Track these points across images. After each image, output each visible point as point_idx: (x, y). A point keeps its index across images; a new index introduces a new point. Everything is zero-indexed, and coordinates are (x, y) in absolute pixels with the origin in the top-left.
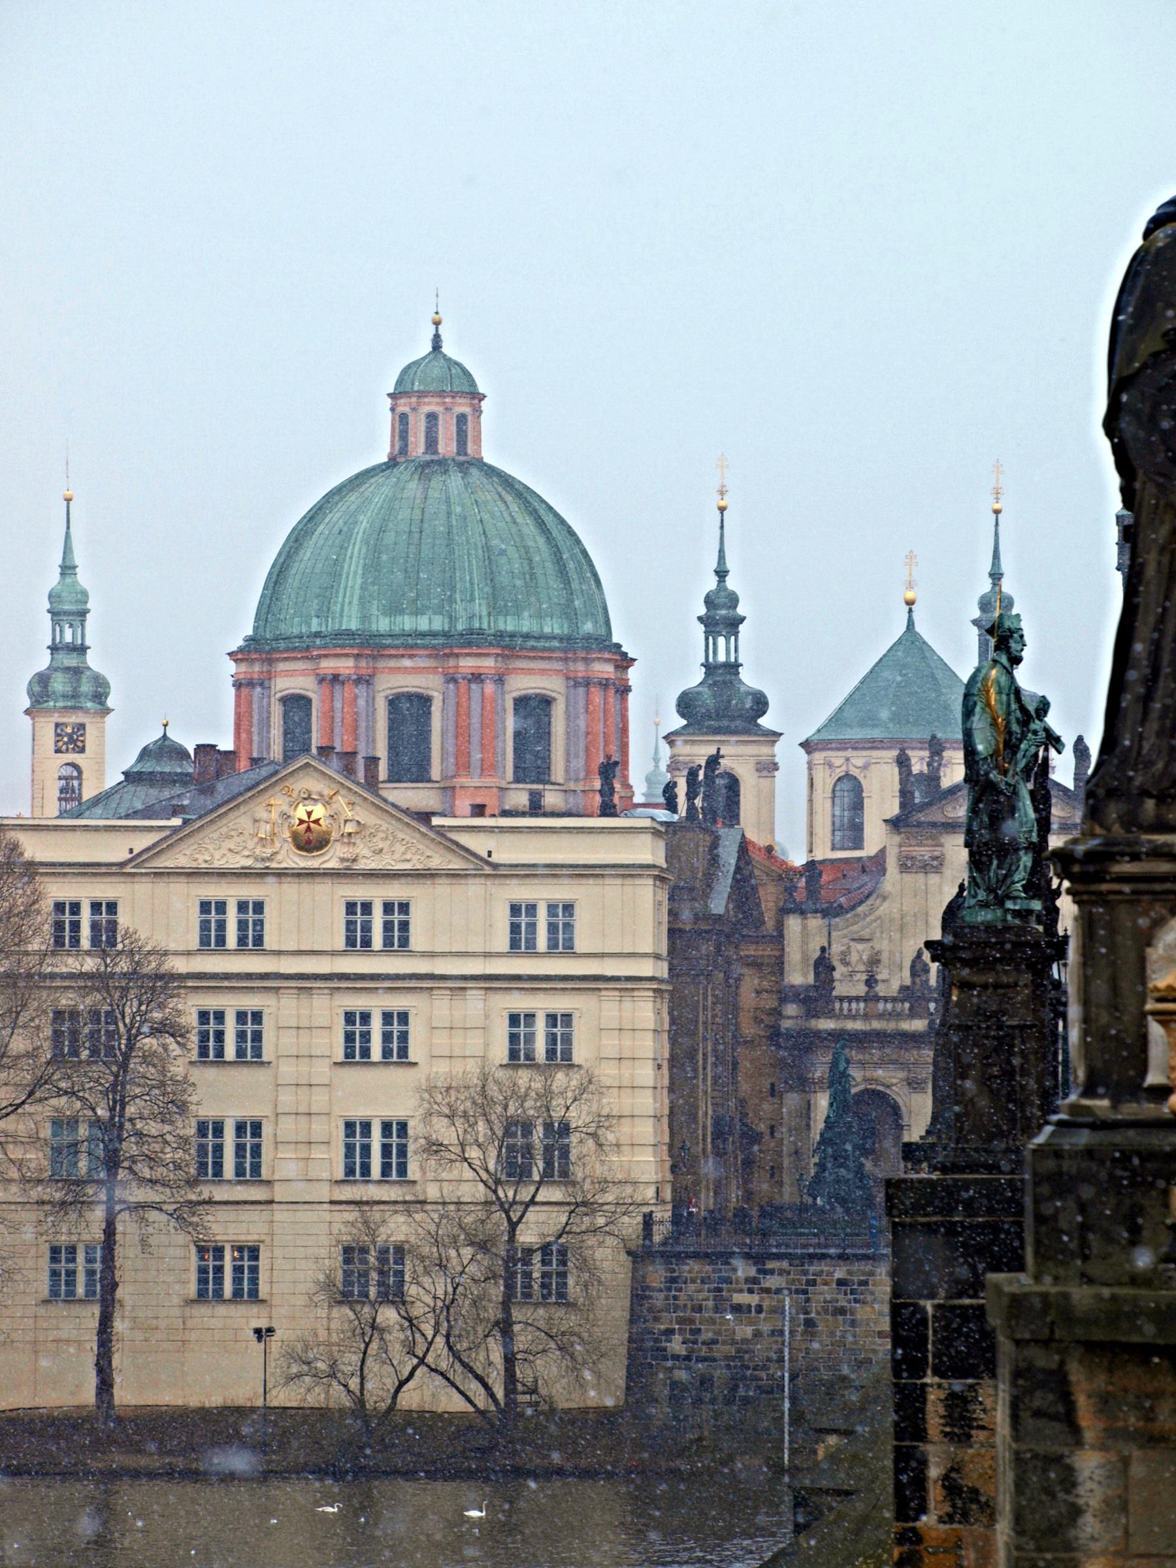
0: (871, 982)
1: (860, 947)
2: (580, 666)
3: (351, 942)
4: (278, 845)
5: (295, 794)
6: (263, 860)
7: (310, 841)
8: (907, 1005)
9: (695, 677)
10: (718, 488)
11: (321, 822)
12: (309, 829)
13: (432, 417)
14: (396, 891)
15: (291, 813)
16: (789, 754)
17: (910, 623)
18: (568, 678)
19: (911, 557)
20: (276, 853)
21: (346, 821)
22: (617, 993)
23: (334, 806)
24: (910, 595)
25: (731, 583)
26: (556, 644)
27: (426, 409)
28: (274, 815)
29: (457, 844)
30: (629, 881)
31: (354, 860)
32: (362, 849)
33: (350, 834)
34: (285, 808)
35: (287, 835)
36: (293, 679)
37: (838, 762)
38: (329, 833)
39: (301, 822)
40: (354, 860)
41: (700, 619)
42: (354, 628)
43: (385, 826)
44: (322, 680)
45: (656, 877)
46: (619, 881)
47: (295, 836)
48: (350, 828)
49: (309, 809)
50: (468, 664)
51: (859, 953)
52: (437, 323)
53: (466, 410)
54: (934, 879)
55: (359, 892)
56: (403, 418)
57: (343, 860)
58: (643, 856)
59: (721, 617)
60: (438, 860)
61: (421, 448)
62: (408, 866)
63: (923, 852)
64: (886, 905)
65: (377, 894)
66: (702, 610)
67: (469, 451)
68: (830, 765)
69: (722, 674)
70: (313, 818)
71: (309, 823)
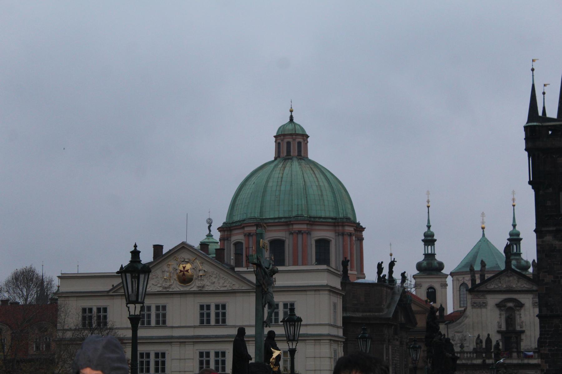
0: (462, 347)
1: (459, 334)
2: (340, 228)
3: (202, 322)
4: (172, 282)
5: (179, 260)
6: (166, 288)
7: (185, 279)
8: (475, 355)
9: (422, 258)
10: (426, 200)
11: (189, 271)
12: (184, 274)
13: (289, 144)
14: (220, 300)
15: (177, 268)
16: (449, 280)
17: (484, 235)
18: (336, 233)
19: (483, 214)
20: (171, 285)
21: (199, 271)
22: (313, 341)
23: (195, 264)
24: (483, 226)
25: (431, 229)
26: (330, 220)
27: (286, 140)
28: (171, 269)
29: (245, 278)
30: (317, 293)
31: (203, 287)
32: (206, 282)
33: (201, 276)
34: (175, 266)
35: (175, 277)
36: (238, 237)
37: (460, 279)
38: (193, 276)
39: (181, 271)
40: (203, 287)
41: (423, 240)
42: (256, 216)
43: (216, 272)
44: (245, 235)
45: (330, 291)
46: (313, 293)
47: (179, 277)
48: (201, 273)
49: (184, 265)
50: (296, 227)
51: (458, 336)
52: (291, 111)
53: (301, 140)
54: (484, 310)
55: (205, 300)
56: (279, 144)
57: (198, 287)
58: (324, 282)
59: (429, 240)
60: (237, 286)
61: (285, 154)
62: (225, 289)
63: (480, 300)
64: (467, 319)
65: (213, 301)
66: (423, 238)
67: (302, 155)
68: (458, 280)
69: (430, 257)
70: (186, 269)
71: (184, 271)
